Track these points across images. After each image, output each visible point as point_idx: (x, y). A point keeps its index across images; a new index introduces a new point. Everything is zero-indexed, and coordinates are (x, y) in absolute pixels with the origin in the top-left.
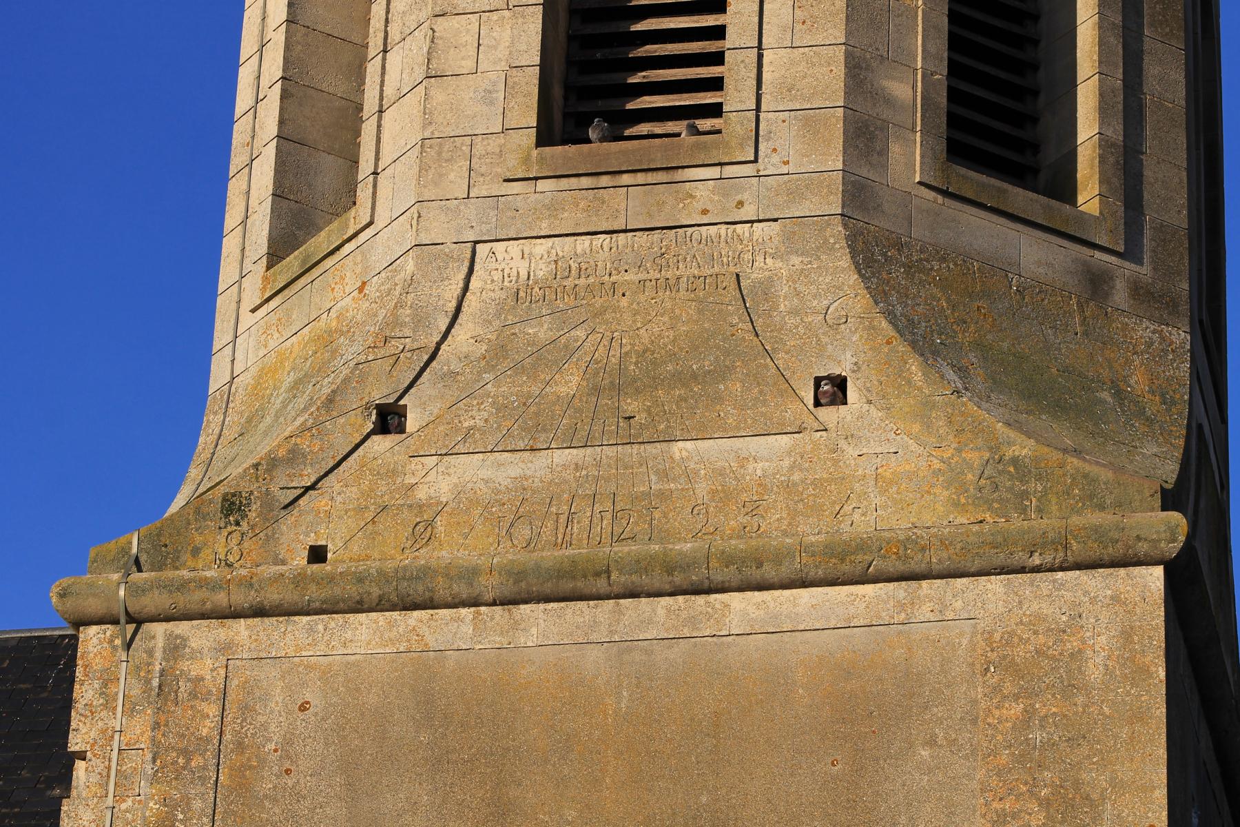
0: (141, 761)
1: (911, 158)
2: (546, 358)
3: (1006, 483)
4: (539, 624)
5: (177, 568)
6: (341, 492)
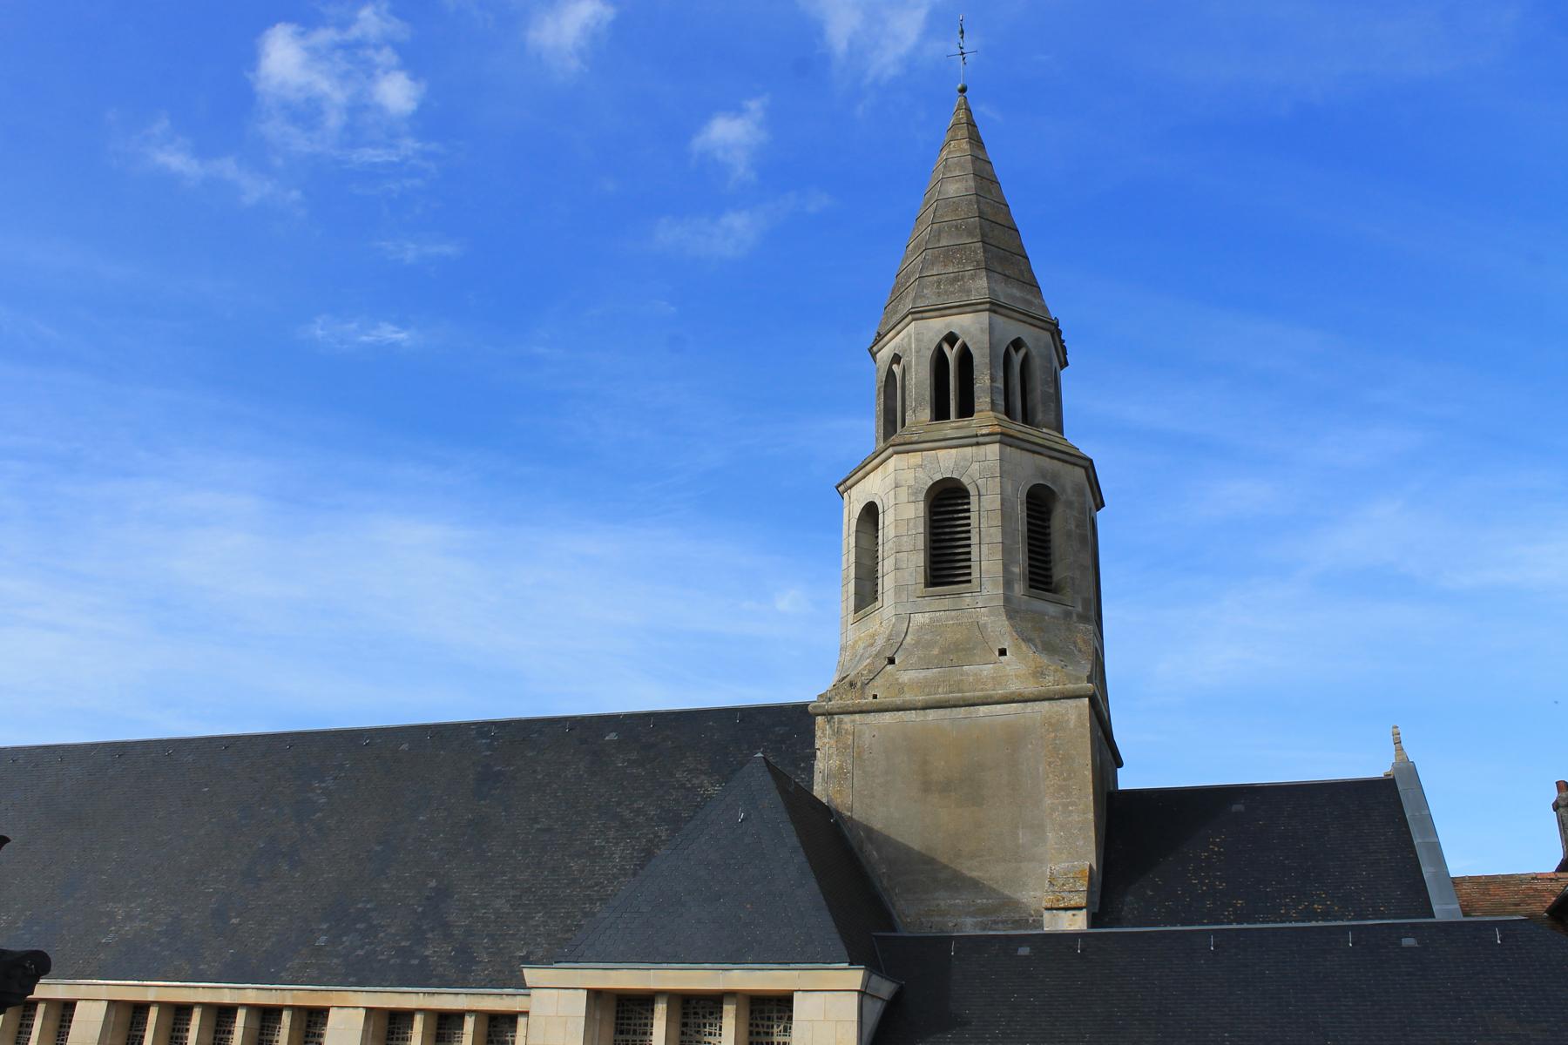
0: (833, 750)
1: (1019, 588)
2: (929, 645)
3: (1039, 674)
4: (932, 715)
5: (981, 628)
6: (879, 681)
